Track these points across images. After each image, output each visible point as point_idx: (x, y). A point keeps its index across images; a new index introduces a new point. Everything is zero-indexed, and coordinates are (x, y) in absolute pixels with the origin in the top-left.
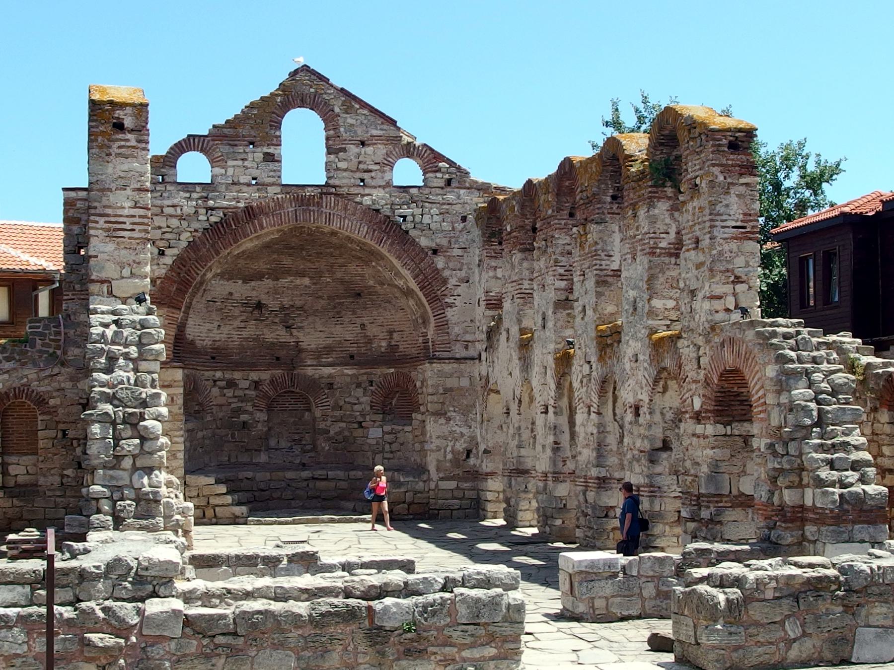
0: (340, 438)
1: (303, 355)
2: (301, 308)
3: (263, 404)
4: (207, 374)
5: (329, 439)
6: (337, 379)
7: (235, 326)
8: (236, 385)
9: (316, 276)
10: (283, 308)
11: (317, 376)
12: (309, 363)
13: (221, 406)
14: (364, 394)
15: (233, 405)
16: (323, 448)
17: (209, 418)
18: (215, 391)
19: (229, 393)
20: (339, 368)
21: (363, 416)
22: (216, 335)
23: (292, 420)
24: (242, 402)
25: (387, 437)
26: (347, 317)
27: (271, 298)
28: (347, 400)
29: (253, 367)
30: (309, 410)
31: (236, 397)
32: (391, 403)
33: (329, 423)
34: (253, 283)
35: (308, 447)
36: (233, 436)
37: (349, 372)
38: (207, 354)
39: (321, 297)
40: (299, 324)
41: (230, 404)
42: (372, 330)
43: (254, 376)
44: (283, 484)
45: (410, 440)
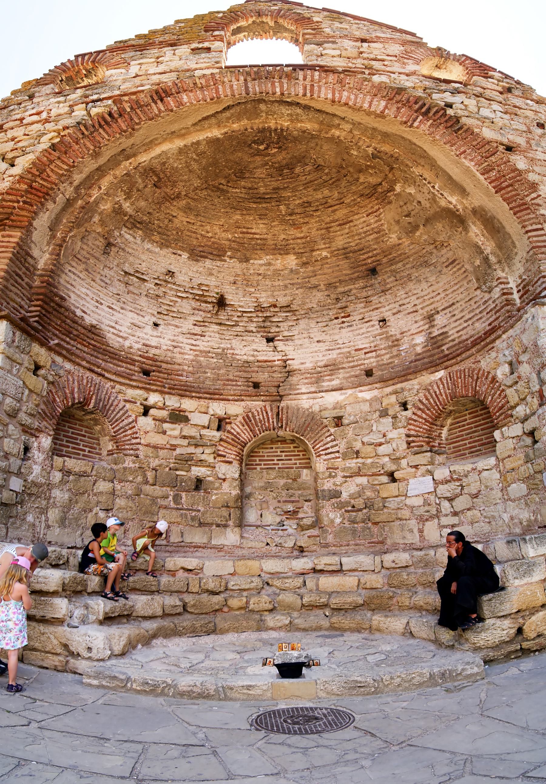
0: (359, 503)
1: (294, 379)
2: (287, 308)
3: (231, 454)
4: (131, 393)
5: (341, 506)
6: (349, 409)
7: (185, 330)
8: (186, 420)
9: (306, 251)
10: (259, 308)
11: (316, 408)
12: (304, 390)
13: (155, 447)
14: (395, 427)
15: (178, 451)
16: (332, 521)
17: (129, 463)
18: (145, 423)
19: (174, 430)
20: (350, 392)
21: (396, 460)
22: (149, 335)
23: (282, 482)
24: (196, 446)
25: (443, 490)
26: (358, 310)
27: (241, 293)
28: (365, 440)
29: (214, 395)
30: (309, 467)
31: (185, 437)
32: (439, 436)
33: (339, 480)
34: (208, 263)
35: (307, 521)
36: (177, 498)
37: (367, 394)
38: (133, 362)
39: (316, 287)
40: (286, 334)
41: (173, 448)
42: (397, 325)
43: (218, 408)
44: (257, 582)
45: (494, 484)
